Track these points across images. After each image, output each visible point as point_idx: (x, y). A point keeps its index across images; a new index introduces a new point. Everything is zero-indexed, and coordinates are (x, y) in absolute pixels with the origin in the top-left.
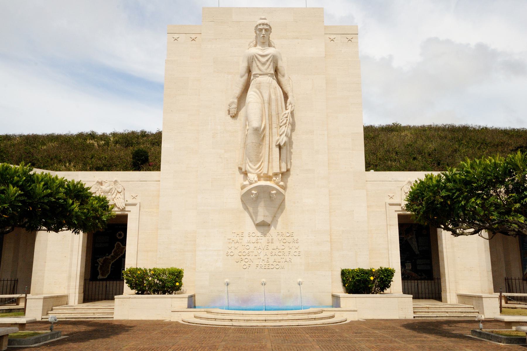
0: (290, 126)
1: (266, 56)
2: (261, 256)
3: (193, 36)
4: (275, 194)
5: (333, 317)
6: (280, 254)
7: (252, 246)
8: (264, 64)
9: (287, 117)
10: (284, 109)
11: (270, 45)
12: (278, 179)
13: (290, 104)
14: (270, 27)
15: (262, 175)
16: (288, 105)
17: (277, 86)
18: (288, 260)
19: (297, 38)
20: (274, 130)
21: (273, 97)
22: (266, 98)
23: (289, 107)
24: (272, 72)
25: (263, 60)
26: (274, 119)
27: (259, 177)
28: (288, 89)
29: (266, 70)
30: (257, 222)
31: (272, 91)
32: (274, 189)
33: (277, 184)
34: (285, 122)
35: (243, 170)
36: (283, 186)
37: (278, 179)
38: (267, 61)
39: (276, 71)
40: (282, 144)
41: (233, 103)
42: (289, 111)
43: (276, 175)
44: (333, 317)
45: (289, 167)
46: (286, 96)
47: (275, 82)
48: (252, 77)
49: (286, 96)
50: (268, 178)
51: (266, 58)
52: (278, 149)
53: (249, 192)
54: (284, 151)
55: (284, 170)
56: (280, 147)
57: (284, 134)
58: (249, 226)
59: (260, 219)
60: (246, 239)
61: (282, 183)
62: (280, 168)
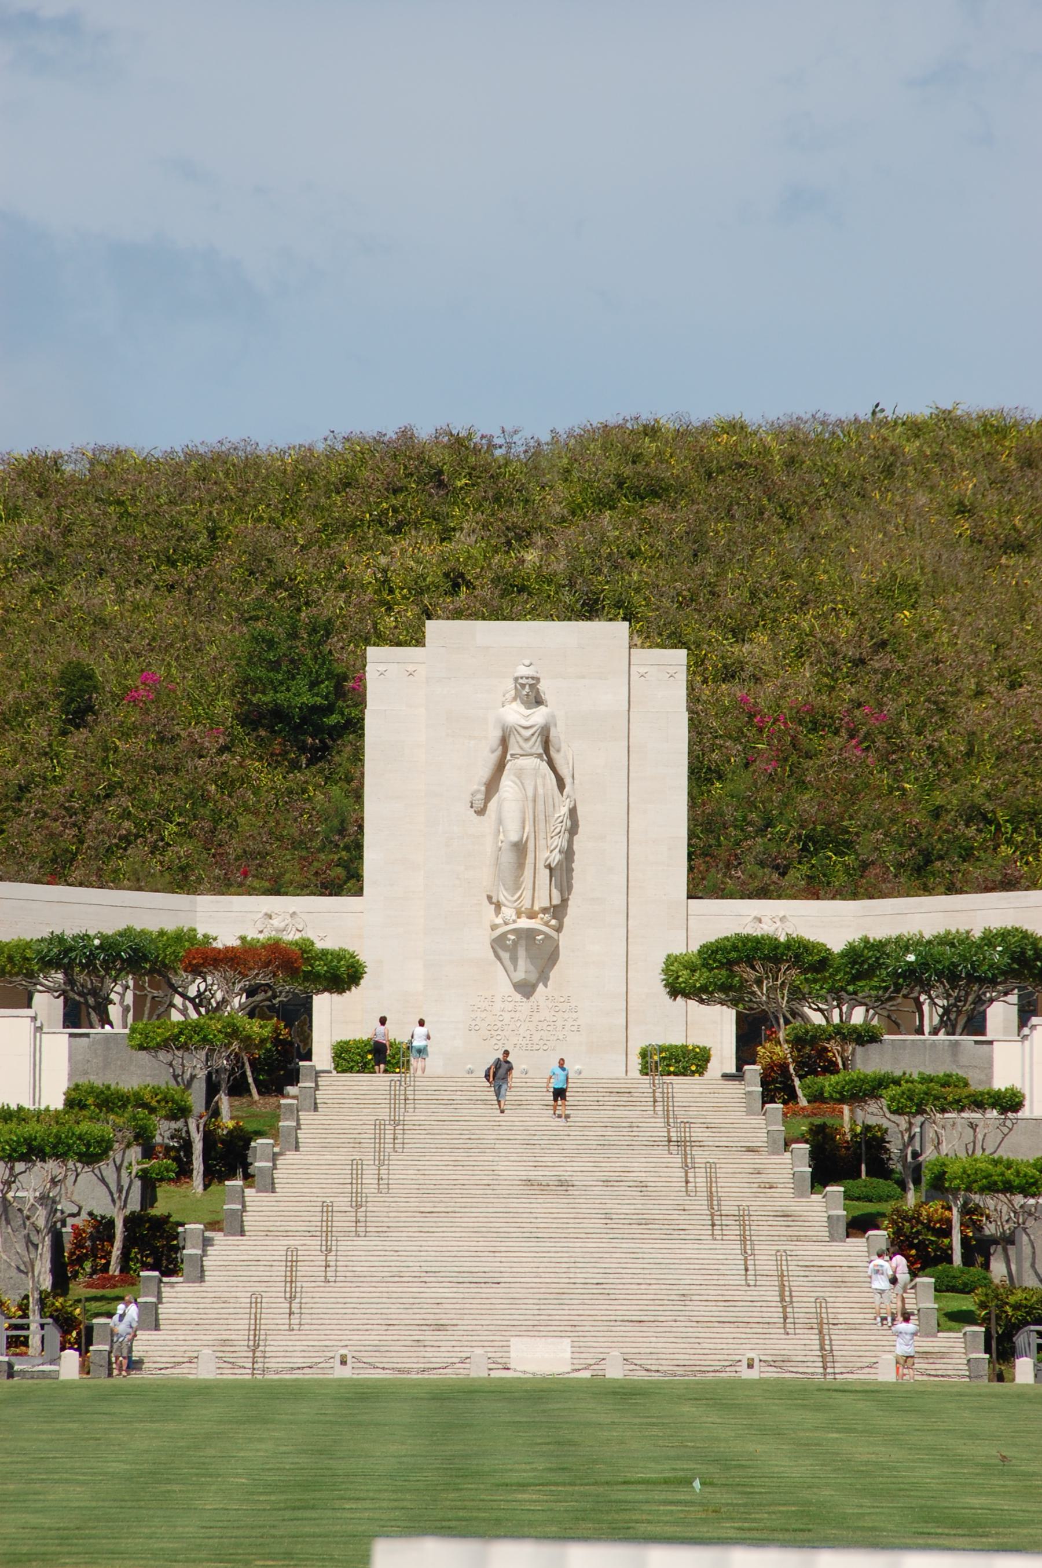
0: (567, 835)
2: (522, 1031)
4: (542, 940)
6: (549, 1028)
7: (507, 1016)
8: (527, 740)
18: (561, 1038)
19: (583, 677)
20: (542, 843)
21: (540, 791)
22: (530, 794)
24: (541, 751)
25: (527, 733)
26: (541, 825)
27: (519, 915)
30: (515, 981)
31: (539, 781)
33: (546, 924)
34: (558, 830)
39: (546, 744)
40: (553, 866)
41: (478, 791)
43: (545, 910)
46: (561, 784)
47: (544, 765)
48: (508, 757)
49: (561, 784)
51: (531, 731)
53: (503, 936)
57: (557, 850)
58: (504, 987)
59: (520, 975)
60: (498, 1005)
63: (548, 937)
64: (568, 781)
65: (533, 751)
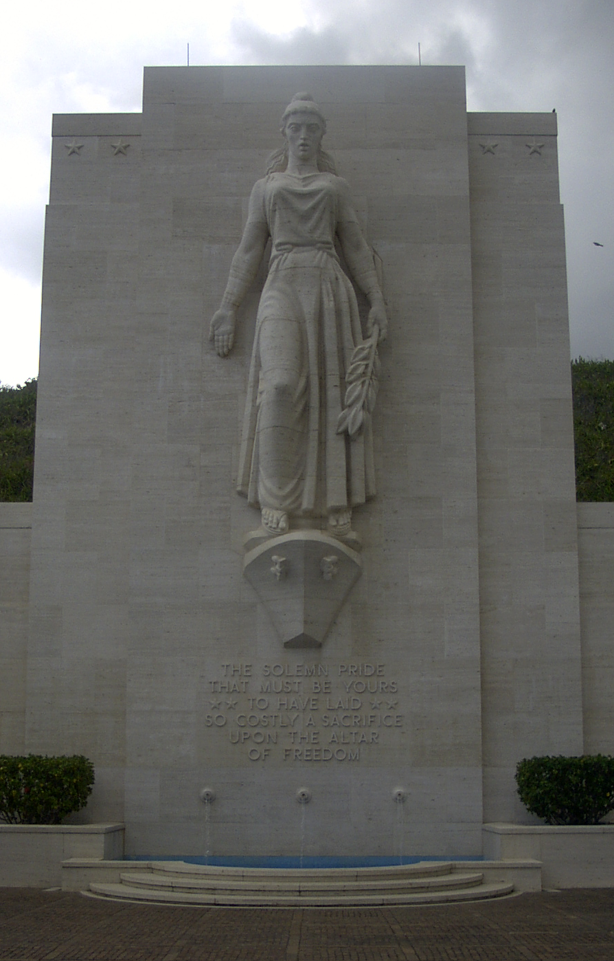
0: (375, 383)
1: (311, 195)
3: (118, 143)
4: (335, 563)
5: (479, 882)
8: (305, 217)
9: (364, 359)
10: (359, 336)
11: (322, 168)
12: (345, 519)
13: (376, 322)
14: (323, 121)
15: (300, 513)
16: (369, 325)
17: (341, 274)
20: (333, 393)
21: (329, 305)
22: (309, 308)
23: (374, 331)
24: (329, 237)
26: (332, 364)
27: (293, 521)
28: (371, 281)
29: (313, 230)
31: (327, 287)
32: (330, 550)
33: (340, 537)
34: (360, 371)
35: (250, 499)
36: (355, 542)
37: (345, 519)
38: (314, 208)
39: (339, 233)
40: (351, 431)
41: (221, 319)
42: (372, 341)
43: (337, 511)
44: (479, 882)
45: (373, 491)
46: (364, 300)
47: (334, 268)
49: (364, 300)
50: (317, 519)
51: (311, 204)
52: (341, 444)
54: (358, 449)
55: (359, 499)
56: (347, 438)
57: (360, 404)
61: (353, 535)
62: (349, 493)
63: (343, 560)
64: (376, 296)
65: (316, 235)
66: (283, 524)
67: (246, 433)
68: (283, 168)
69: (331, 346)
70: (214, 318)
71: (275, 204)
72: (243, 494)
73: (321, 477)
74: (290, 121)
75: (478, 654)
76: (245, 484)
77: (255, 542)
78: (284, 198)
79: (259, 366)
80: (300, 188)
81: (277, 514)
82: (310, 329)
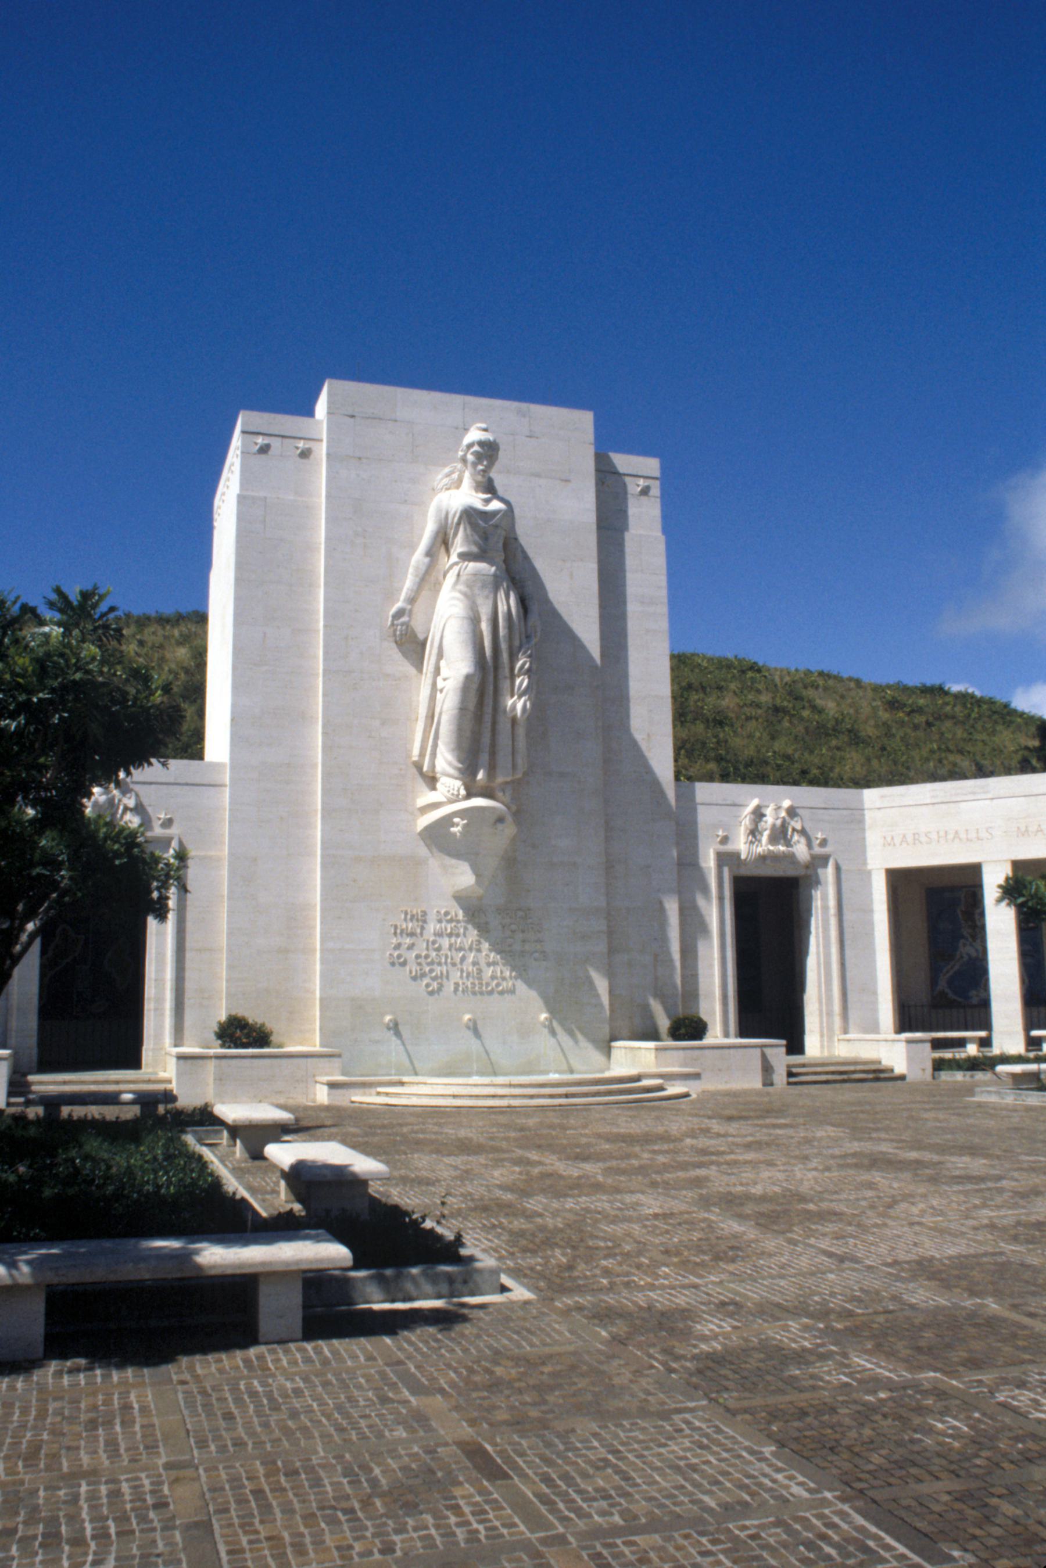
19: (538, 475)
54: (521, 731)
66: (463, 792)
67: (422, 711)
68: (458, 484)
69: (504, 646)
70: (393, 610)
71: (460, 518)
72: (418, 766)
73: (493, 754)
74: (476, 448)
75: (604, 904)
76: (422, 755)
77: (435, 806)
78: (470, 515)
79: (440, 655)
80: (479, 505)
81: (458, 783)
82: (485, 627)
